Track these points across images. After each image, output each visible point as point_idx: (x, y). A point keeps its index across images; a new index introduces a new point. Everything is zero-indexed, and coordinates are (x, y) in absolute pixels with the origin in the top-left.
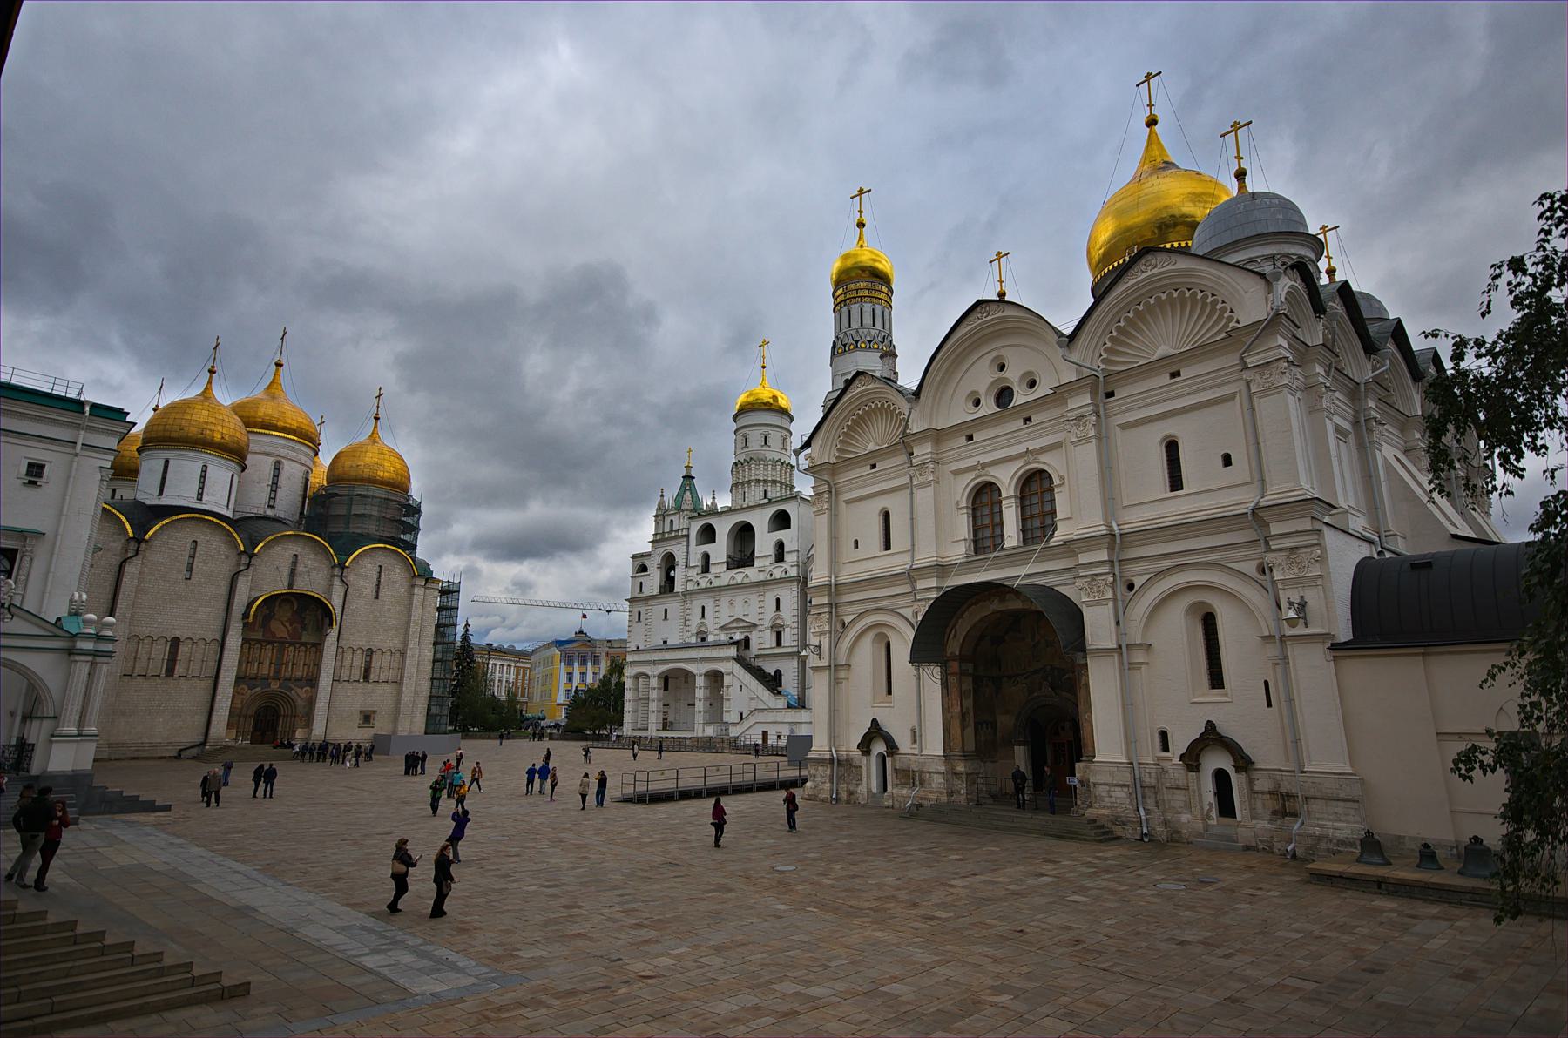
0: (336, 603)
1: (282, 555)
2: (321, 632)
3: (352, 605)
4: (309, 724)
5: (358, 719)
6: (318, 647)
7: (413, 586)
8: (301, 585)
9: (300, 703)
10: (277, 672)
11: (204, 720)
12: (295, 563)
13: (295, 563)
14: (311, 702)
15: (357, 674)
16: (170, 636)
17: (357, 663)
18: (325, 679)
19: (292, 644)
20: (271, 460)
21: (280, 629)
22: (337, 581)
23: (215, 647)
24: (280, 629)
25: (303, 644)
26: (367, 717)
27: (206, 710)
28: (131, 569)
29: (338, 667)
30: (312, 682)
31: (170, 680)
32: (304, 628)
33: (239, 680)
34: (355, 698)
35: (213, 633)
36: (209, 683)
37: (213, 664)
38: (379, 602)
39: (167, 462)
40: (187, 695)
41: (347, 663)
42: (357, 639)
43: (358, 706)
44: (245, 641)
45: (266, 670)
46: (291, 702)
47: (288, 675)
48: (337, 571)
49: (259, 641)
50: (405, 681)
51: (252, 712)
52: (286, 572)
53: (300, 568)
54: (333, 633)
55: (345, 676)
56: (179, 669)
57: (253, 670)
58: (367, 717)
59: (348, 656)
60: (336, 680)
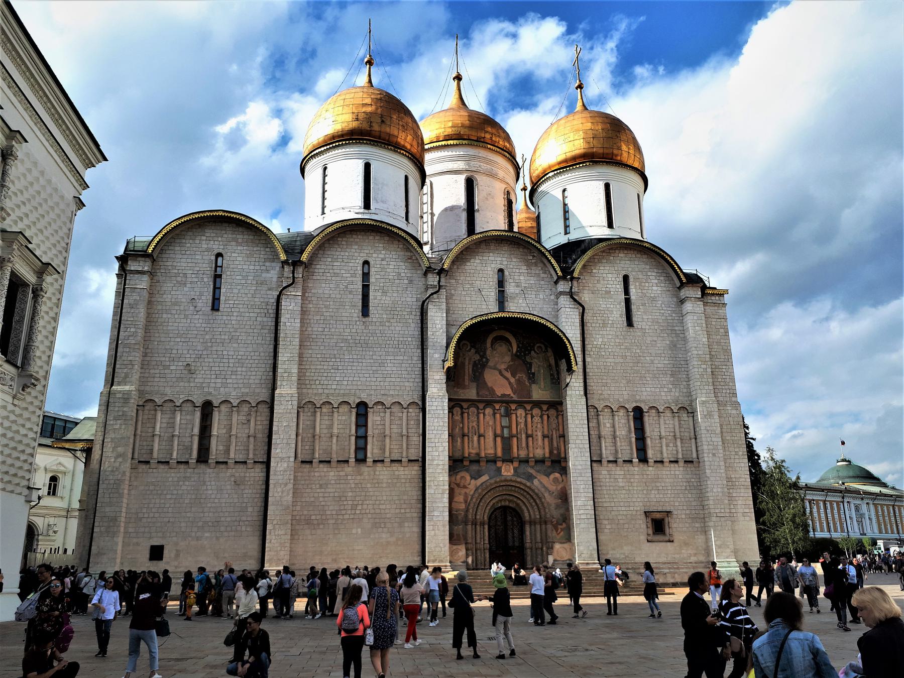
0: (570, 329)
1: (483, 269)
2: (557, 384)
3: (596, 339)
4: (569, 538)
5: (643, 527)
6: (557, 406)
7: (682, 302)
8: (517, 307)
9: (550, 500)
10: (507, 448)
11: (417, 530)
12: (501, 283)
13: (501, 283)
14: (564, 498)
15: (627, 449)
16: (354, 401)
17: (622, 432)
18: (578, 458)
19: (520, 404)
20: (462, 179)
21: (500, 383)
22: (564, 301)
23: (414, 412)
24: (500, 383)
25: (537, 404)
26: (659, 526)
27: (416, 514)
28: (291, 306)
29: (594, 439)
30: (558, 463)
31: (364, 469)
32: (532, 378)
33: (456, 464)
34: (635, 490)
35: (410, 394)
36: (415, 469)
37: (416, 440)
38: (636, 333)
39: (325, 169)
40: (386, 485)
41: (606, 430)
42: (616, 391)
43: (639, 507)
44: (454, 404)
45: (490, 447)
46: (535, 497)
47: (523, 454)
48: (563, 286)
49: (473, 403)
50: (707, 458)
51: (483, 515)
52: (492, 294)
53: (510, 289)
54: (575, 385)
55: (607, 453)
56: (372, 451)
57: (470, 448)
58: (659, 526)
59: (606, 420)
60: (596, 461)
